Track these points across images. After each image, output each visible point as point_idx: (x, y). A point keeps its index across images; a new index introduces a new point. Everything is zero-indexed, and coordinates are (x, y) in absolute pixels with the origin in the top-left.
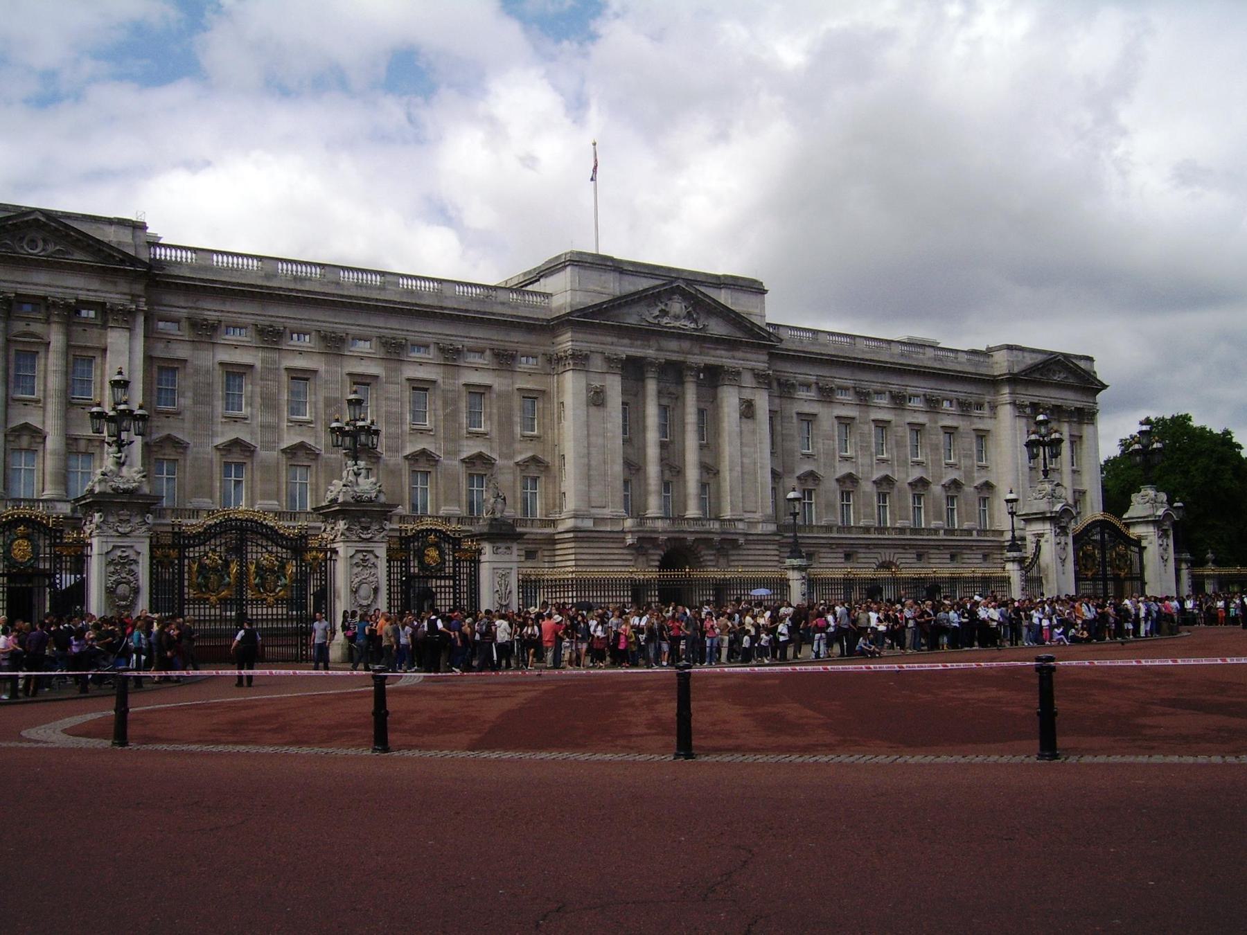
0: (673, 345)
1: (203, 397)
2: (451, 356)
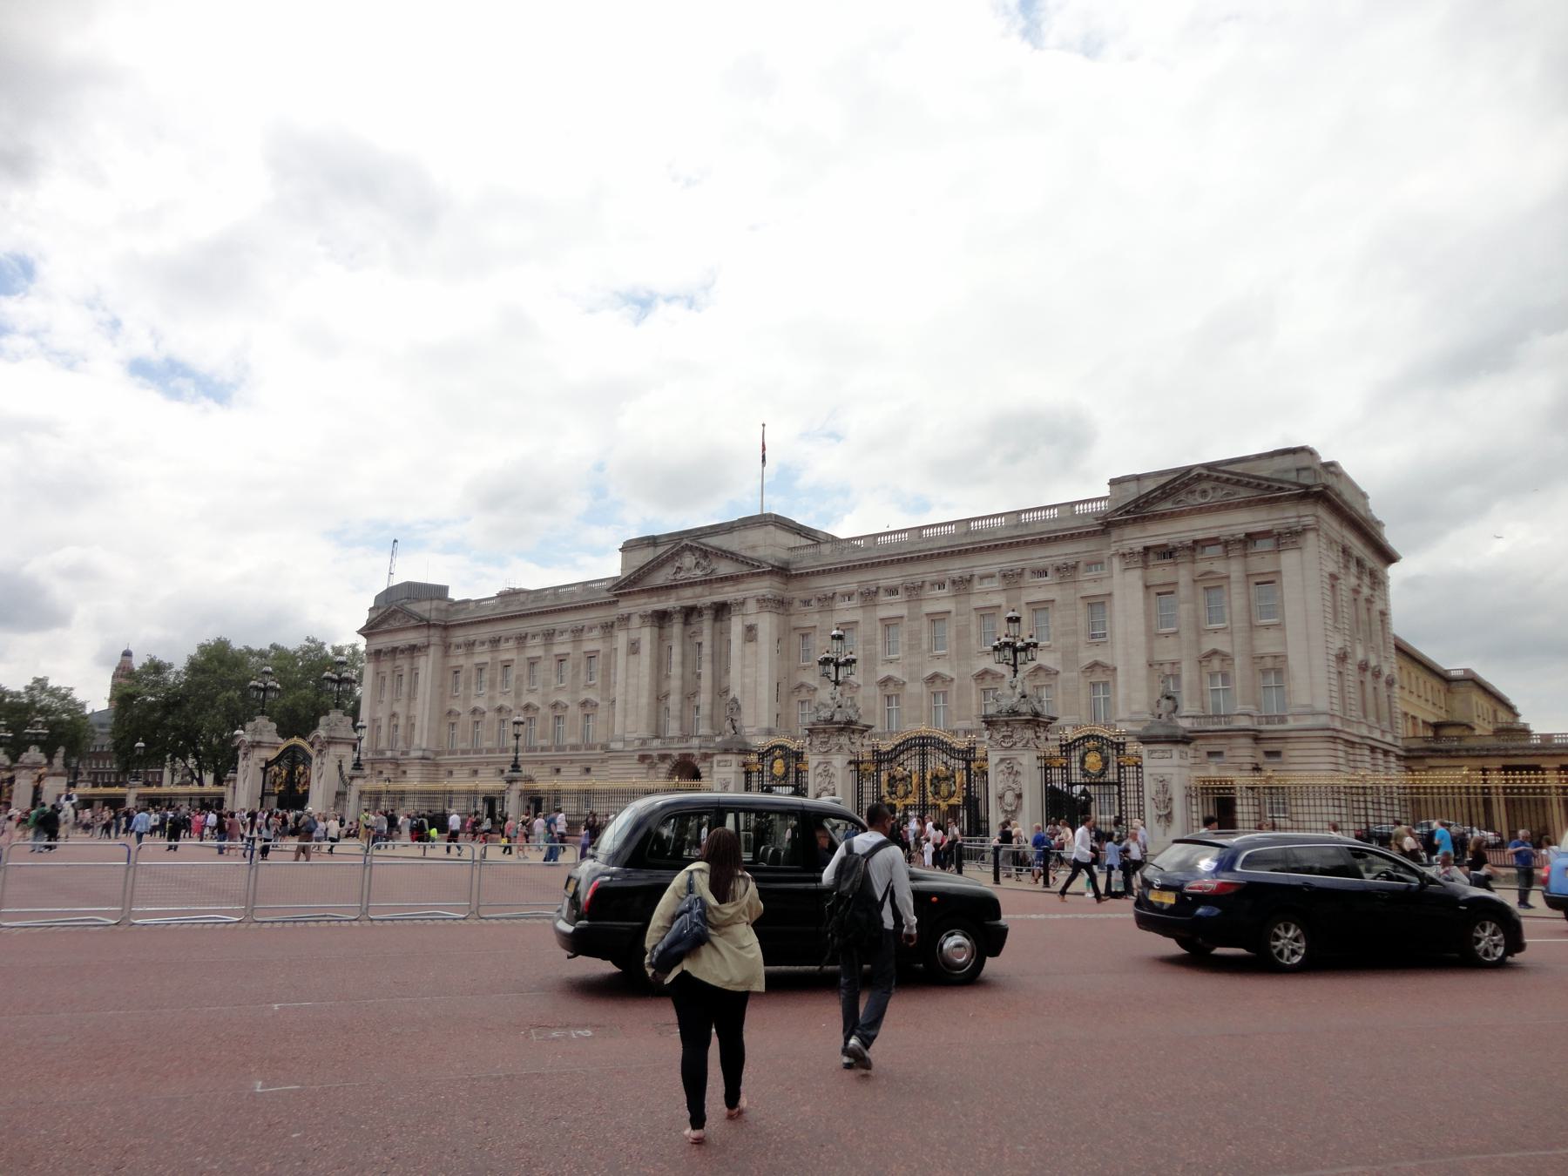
0: (688, 592)
1: (467, 686)
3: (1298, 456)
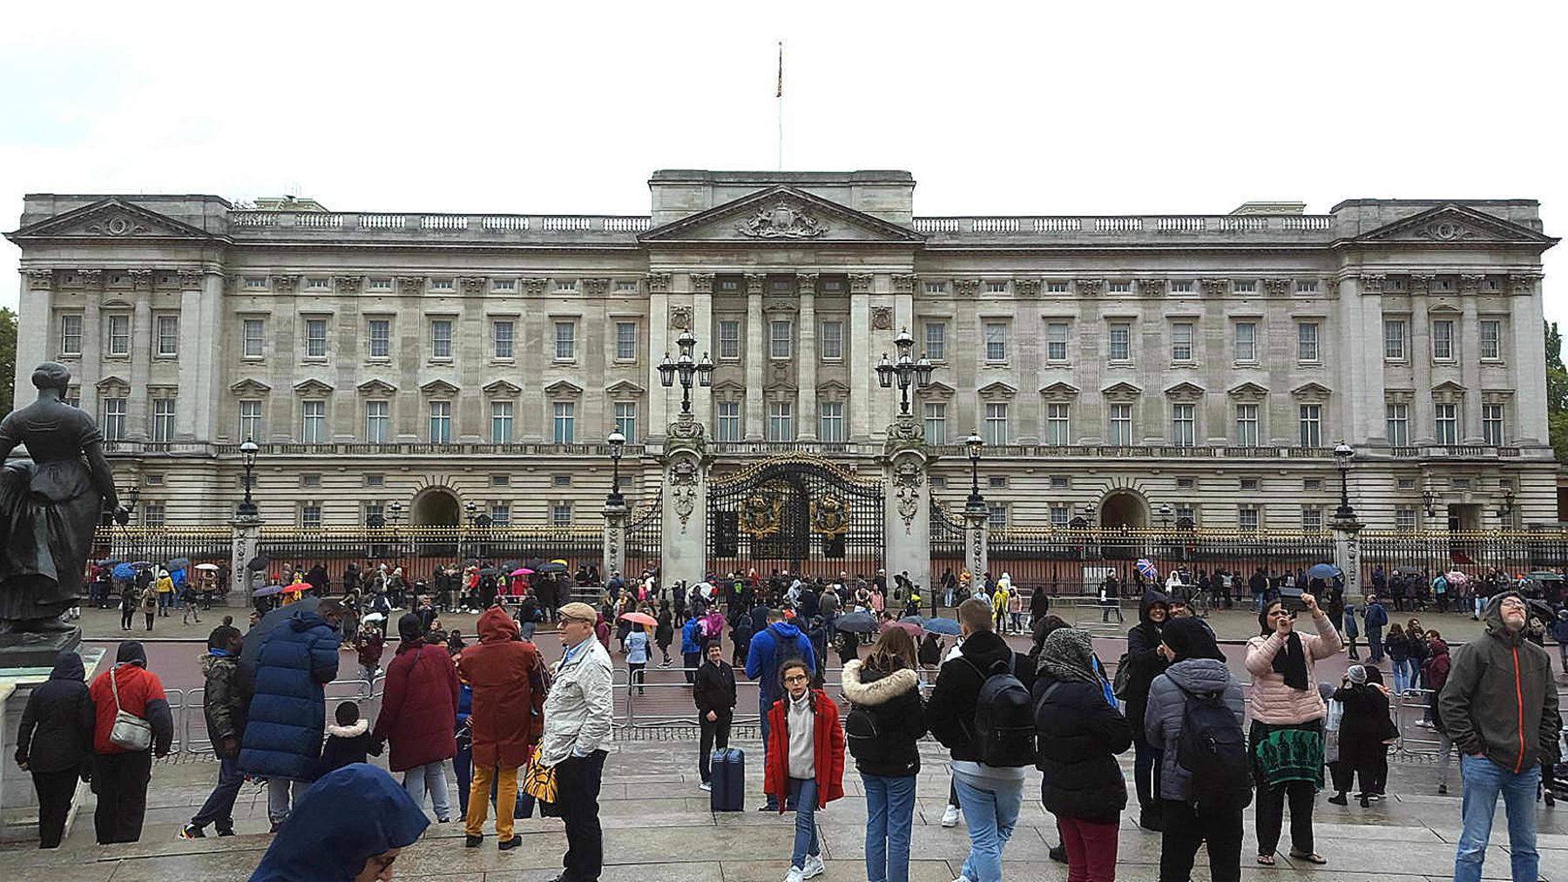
0: (780, 256)
1: (284, 344)
2: (535, 289)
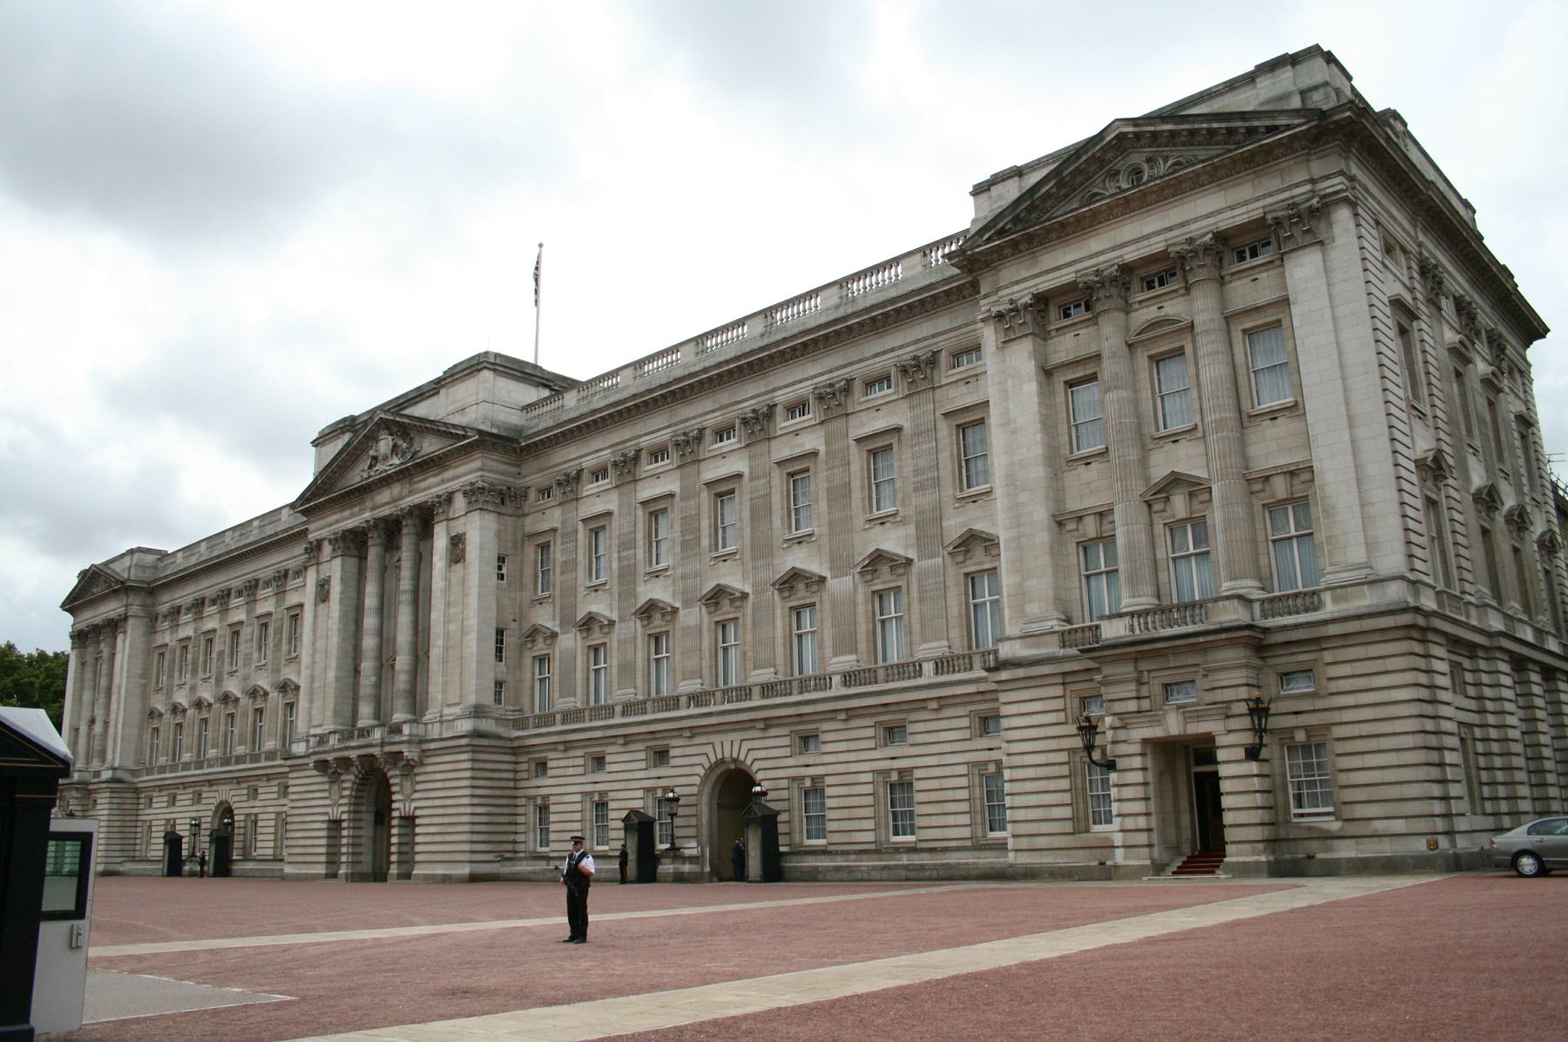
0: (384, 496)
1: (171, 672)
3: (1303, 68)
